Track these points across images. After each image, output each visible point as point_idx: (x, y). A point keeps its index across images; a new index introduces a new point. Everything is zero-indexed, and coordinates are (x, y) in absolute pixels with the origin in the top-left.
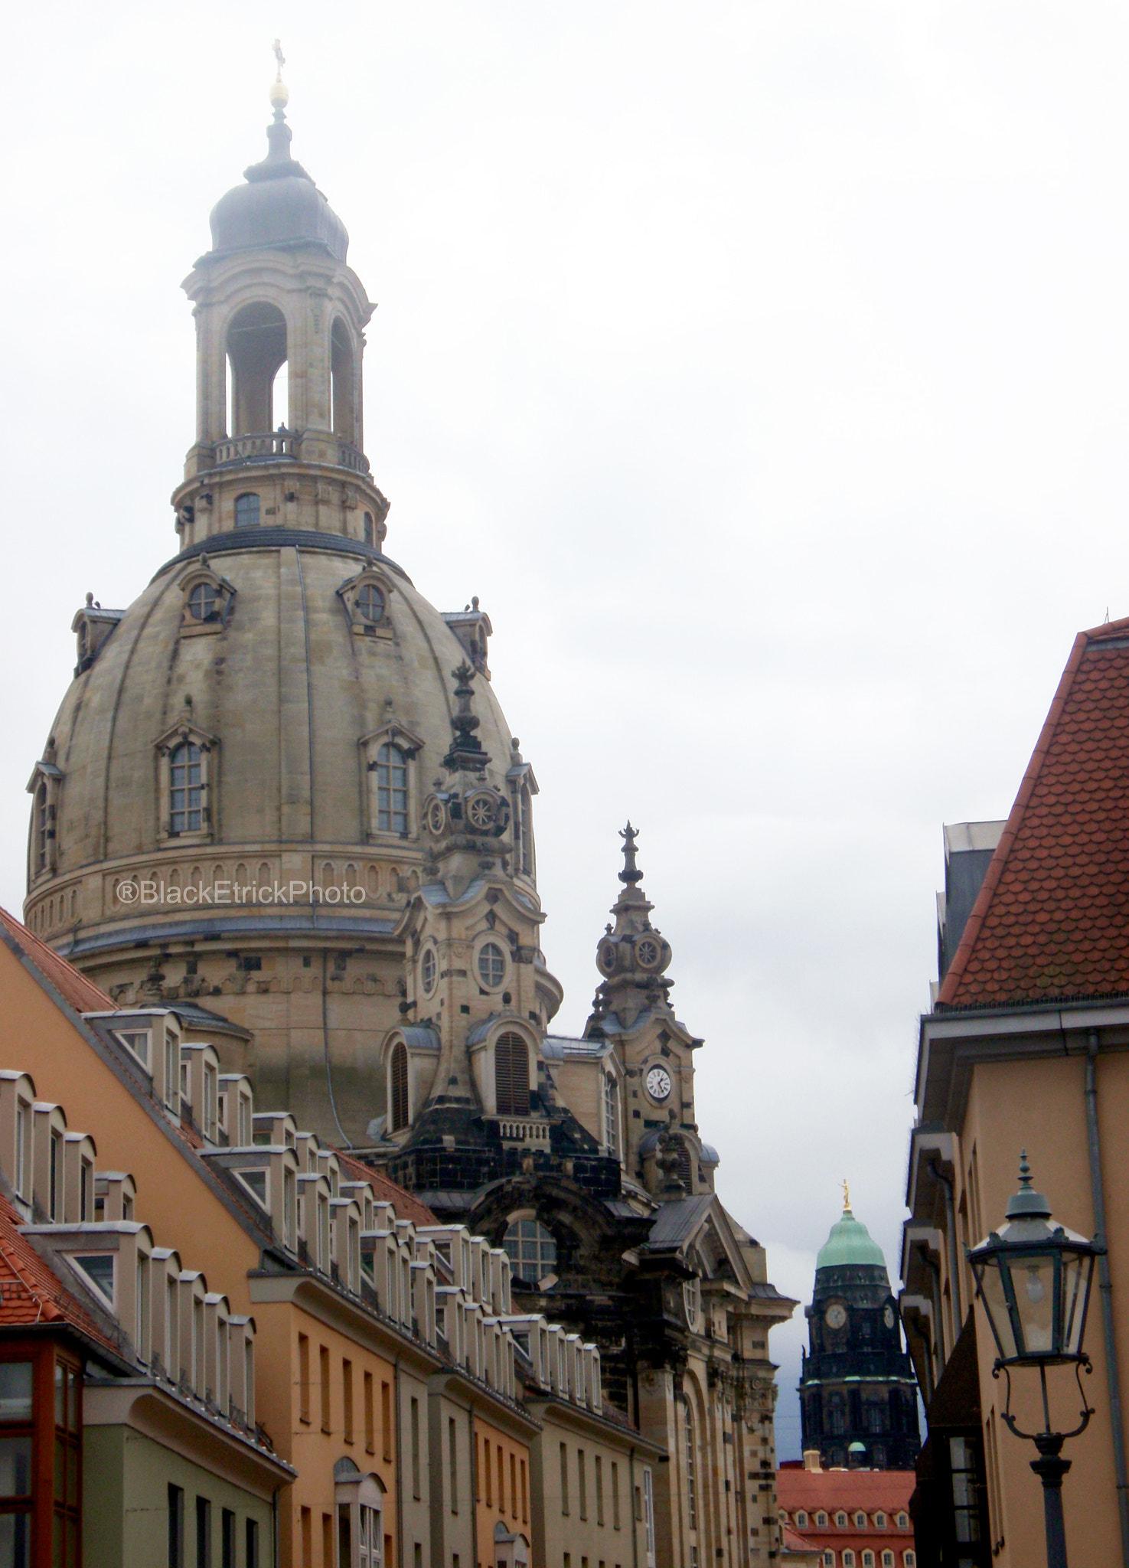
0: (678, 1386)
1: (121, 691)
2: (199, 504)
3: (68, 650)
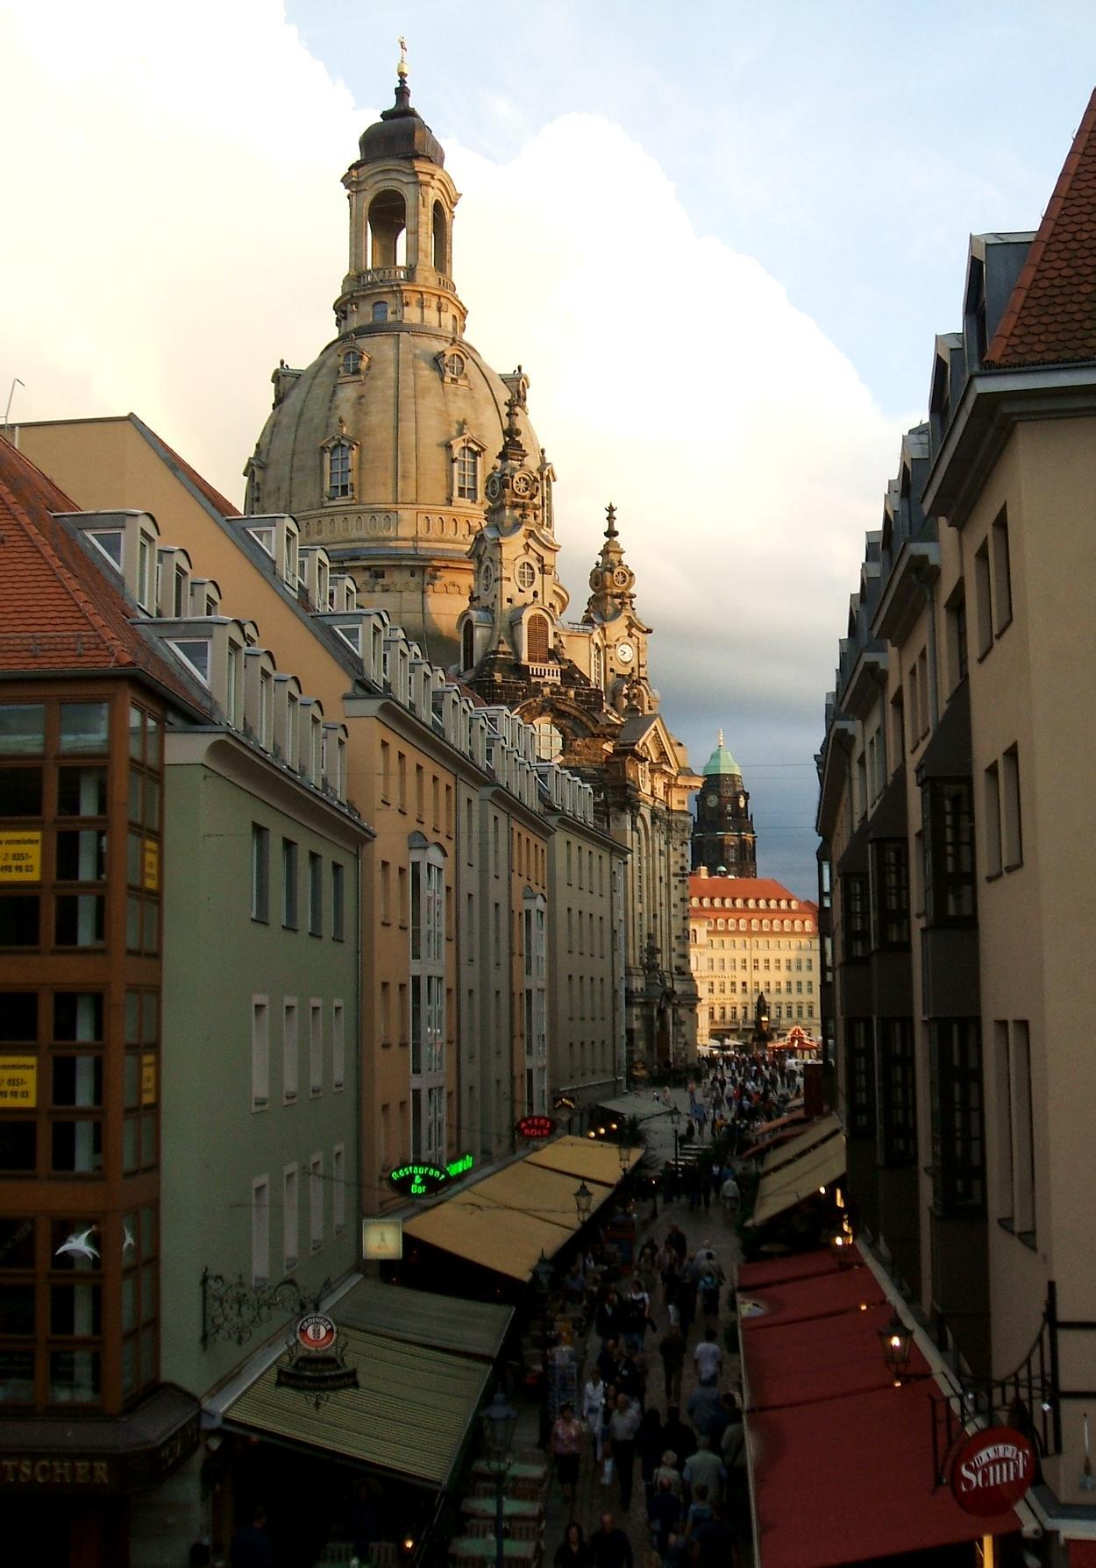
0: (634, 823)
1: (301, 414)
3: (269, 393)
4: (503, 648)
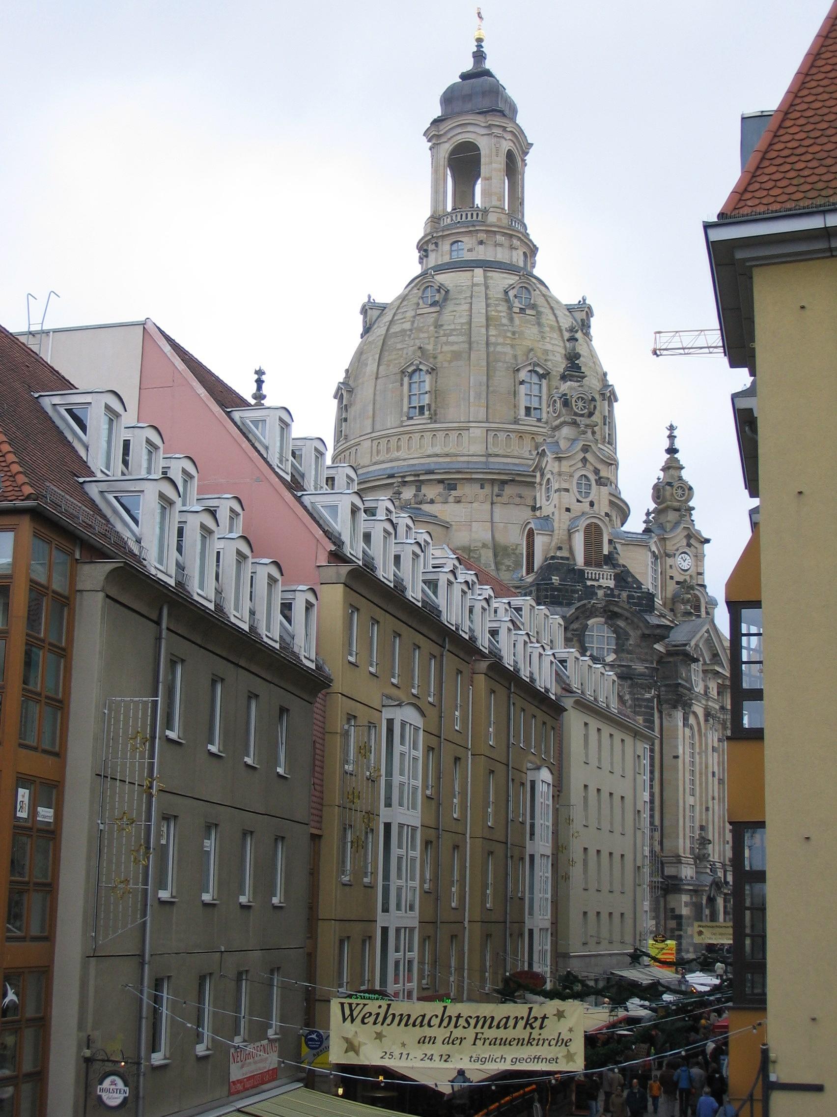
2: (431, 247)
4: (559, 554)
